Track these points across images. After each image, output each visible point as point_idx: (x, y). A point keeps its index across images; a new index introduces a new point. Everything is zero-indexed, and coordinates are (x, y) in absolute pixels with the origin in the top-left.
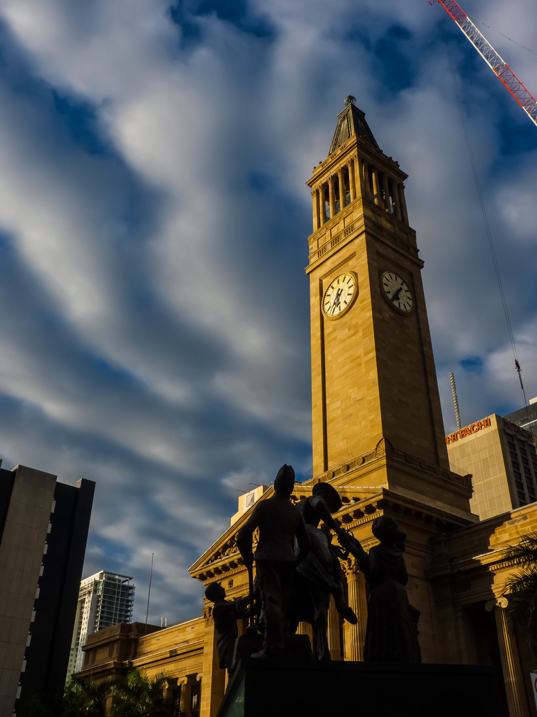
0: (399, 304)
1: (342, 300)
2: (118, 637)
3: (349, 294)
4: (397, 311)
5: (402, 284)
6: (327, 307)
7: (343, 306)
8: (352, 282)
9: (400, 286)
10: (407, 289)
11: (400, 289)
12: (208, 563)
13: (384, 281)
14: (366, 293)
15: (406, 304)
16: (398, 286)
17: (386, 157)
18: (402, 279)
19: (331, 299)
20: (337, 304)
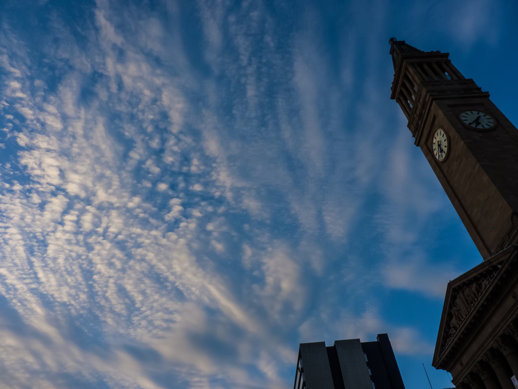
0: (483, 126)
4: (484, 131)
5: (478, 113)
6: (437, 157)
7: (445, 150)
8: (443, 132)
9: (478, 116)
10: (484, 114)
11: (479, 117)
12: (440, 355)
13: (463, 118)
14: (453, 133)
18: (477, 111)
20: (442, 151)
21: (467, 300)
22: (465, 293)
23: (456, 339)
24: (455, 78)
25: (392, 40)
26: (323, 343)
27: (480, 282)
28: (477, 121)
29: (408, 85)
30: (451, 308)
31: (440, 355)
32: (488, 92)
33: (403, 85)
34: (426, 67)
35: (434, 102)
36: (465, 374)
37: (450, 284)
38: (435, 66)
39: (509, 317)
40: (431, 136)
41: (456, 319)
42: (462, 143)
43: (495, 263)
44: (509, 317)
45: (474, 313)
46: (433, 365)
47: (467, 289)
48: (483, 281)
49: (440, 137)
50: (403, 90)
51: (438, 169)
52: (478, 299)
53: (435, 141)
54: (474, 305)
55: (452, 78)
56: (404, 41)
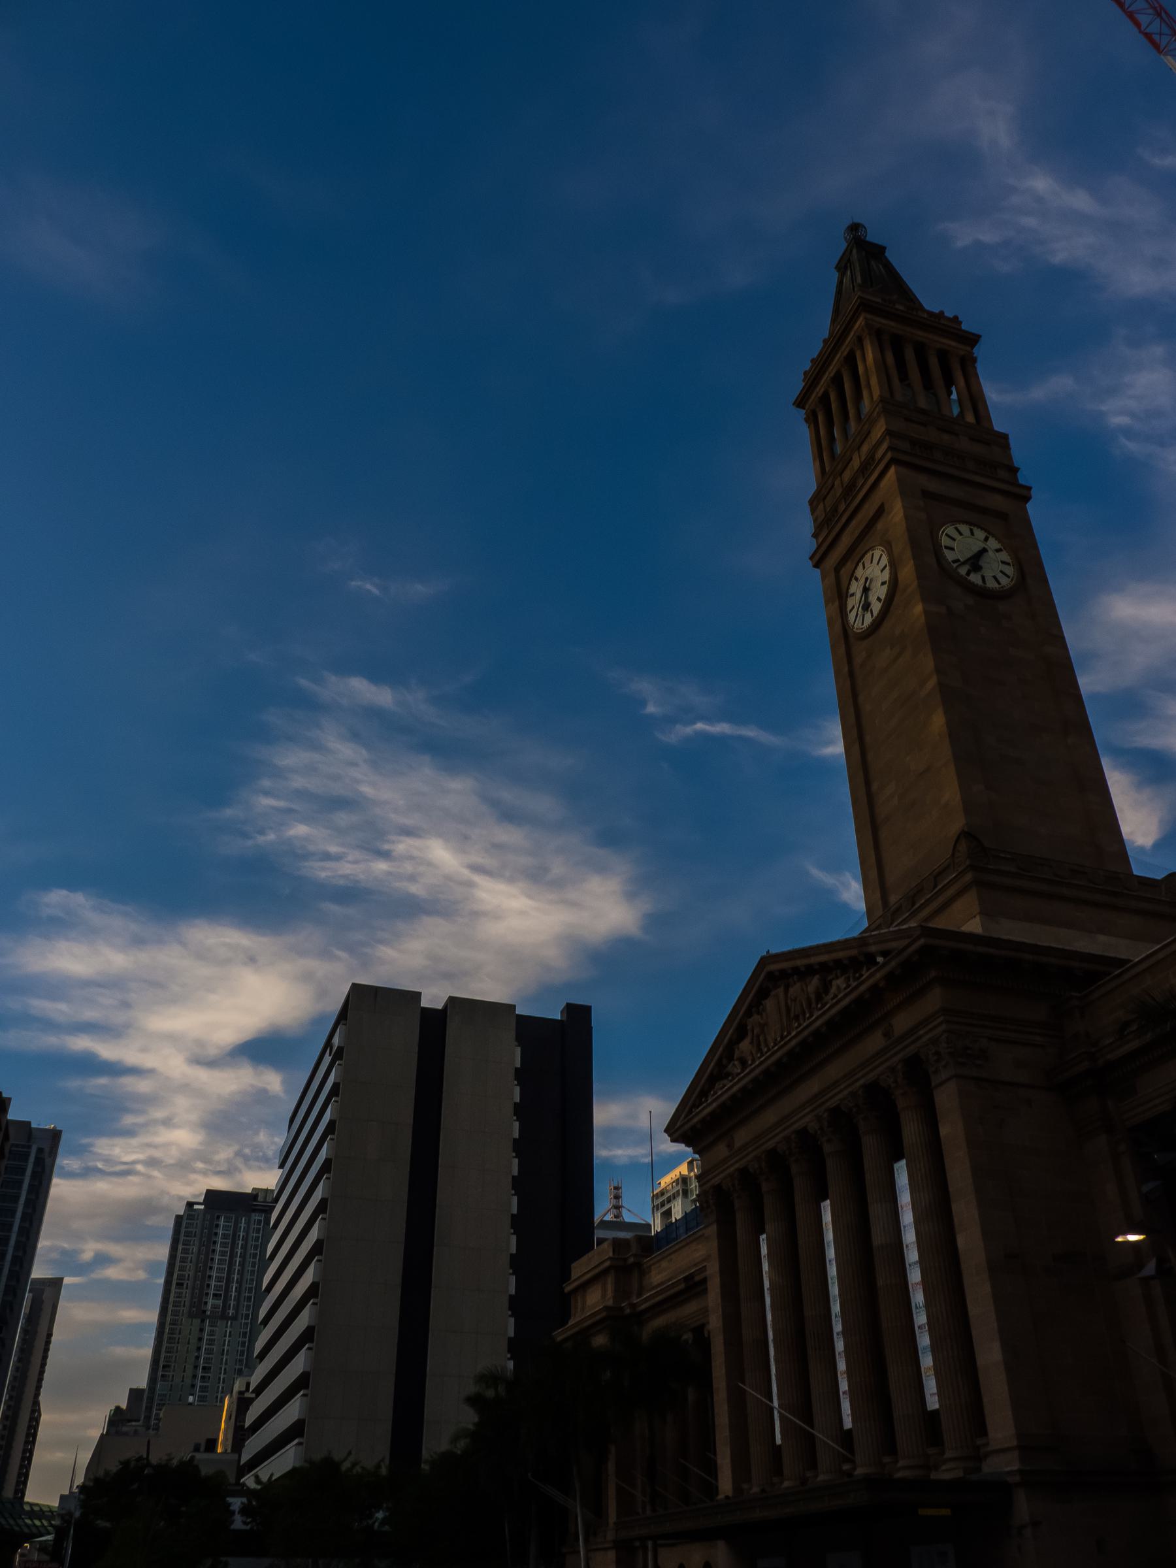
0: (983, 578)
1: (873, 598)
2: (607, 1264)
3: (883, 583)
4: (983, 594)
5: (986, 539)
6: (852, 617)
7: (876, 607)
8: (885, 560)
9: (982, 545)
10: (998, 546)
11: (984, 550)
12: (690, 1112)
13: (945, 541)
14: (908, 572)
15: (1000, 576)
16: (977, 546)
17: (931, 314)
19: (854, 602)
20: (867, 607)
21: (788, 1010)
22: (791, 990)
23: (735, 1089)
24: (970, 418)
25: (855, 228)
26: (418, 995)
27: (830, 978)
28: (975, 562)
29: (847, 386)
30: (749, 1013)
31: (690, 1112)
32: (1030, 488)
33: (837, 380)
34: (910, 354)
35: (892, 470)
36: (728, 1171)
37: (764, 961)
38: (933, 362)
39: (860, 1074)
40: (855, 555)
41: (752, 1043)
42: (919, 608)
43: (873, 949)
44: (860, 1074)
45: (793, 1043)
46: (666, 1131)
47: (798, 985)
48: (837, 978)
49: (875, 570)
50: (833, 396)
51: (842, 650)
52: (811, 1016)
53: (859, 572)
54: (800, 1025)
55: (962, 414)
56: (882, 249)
